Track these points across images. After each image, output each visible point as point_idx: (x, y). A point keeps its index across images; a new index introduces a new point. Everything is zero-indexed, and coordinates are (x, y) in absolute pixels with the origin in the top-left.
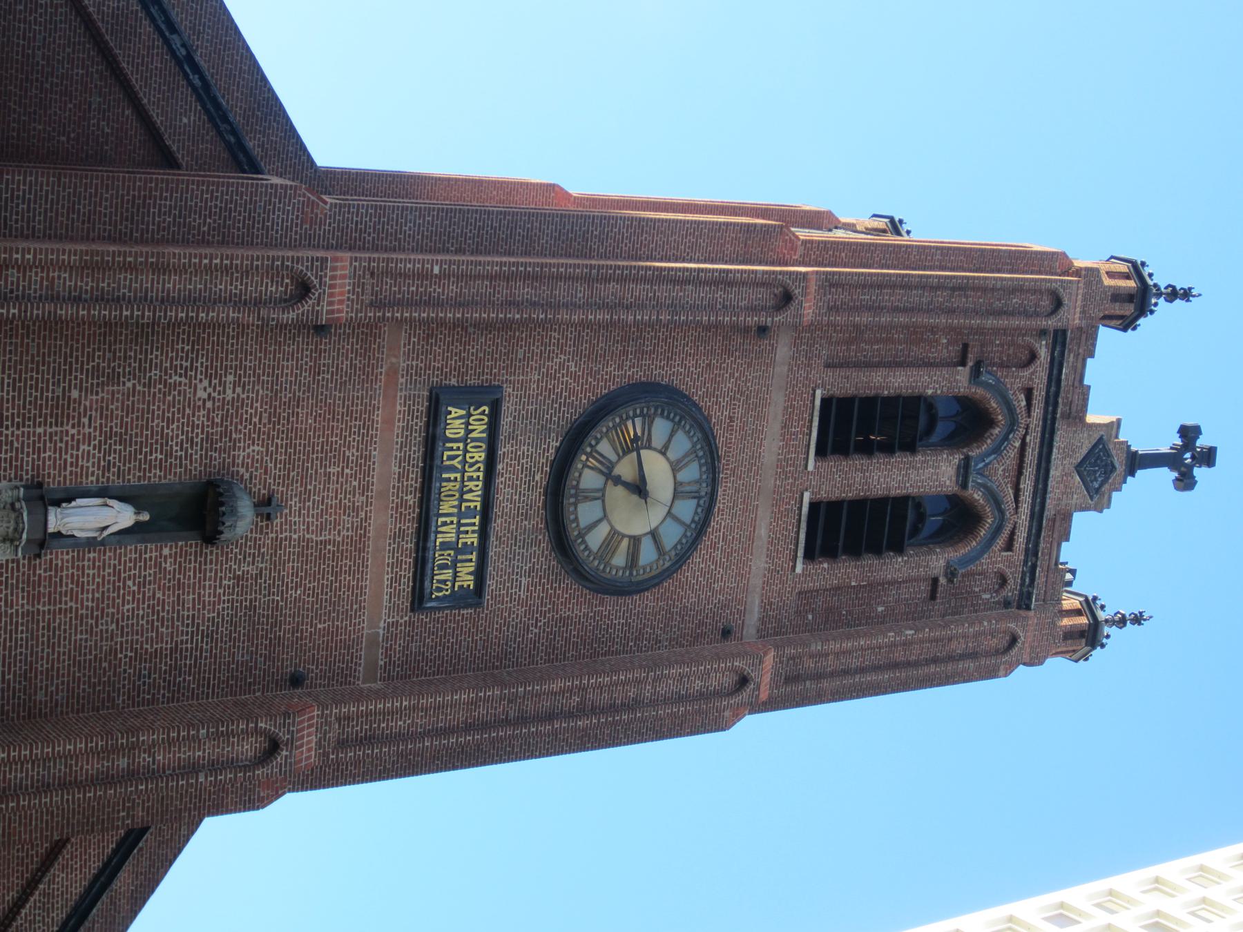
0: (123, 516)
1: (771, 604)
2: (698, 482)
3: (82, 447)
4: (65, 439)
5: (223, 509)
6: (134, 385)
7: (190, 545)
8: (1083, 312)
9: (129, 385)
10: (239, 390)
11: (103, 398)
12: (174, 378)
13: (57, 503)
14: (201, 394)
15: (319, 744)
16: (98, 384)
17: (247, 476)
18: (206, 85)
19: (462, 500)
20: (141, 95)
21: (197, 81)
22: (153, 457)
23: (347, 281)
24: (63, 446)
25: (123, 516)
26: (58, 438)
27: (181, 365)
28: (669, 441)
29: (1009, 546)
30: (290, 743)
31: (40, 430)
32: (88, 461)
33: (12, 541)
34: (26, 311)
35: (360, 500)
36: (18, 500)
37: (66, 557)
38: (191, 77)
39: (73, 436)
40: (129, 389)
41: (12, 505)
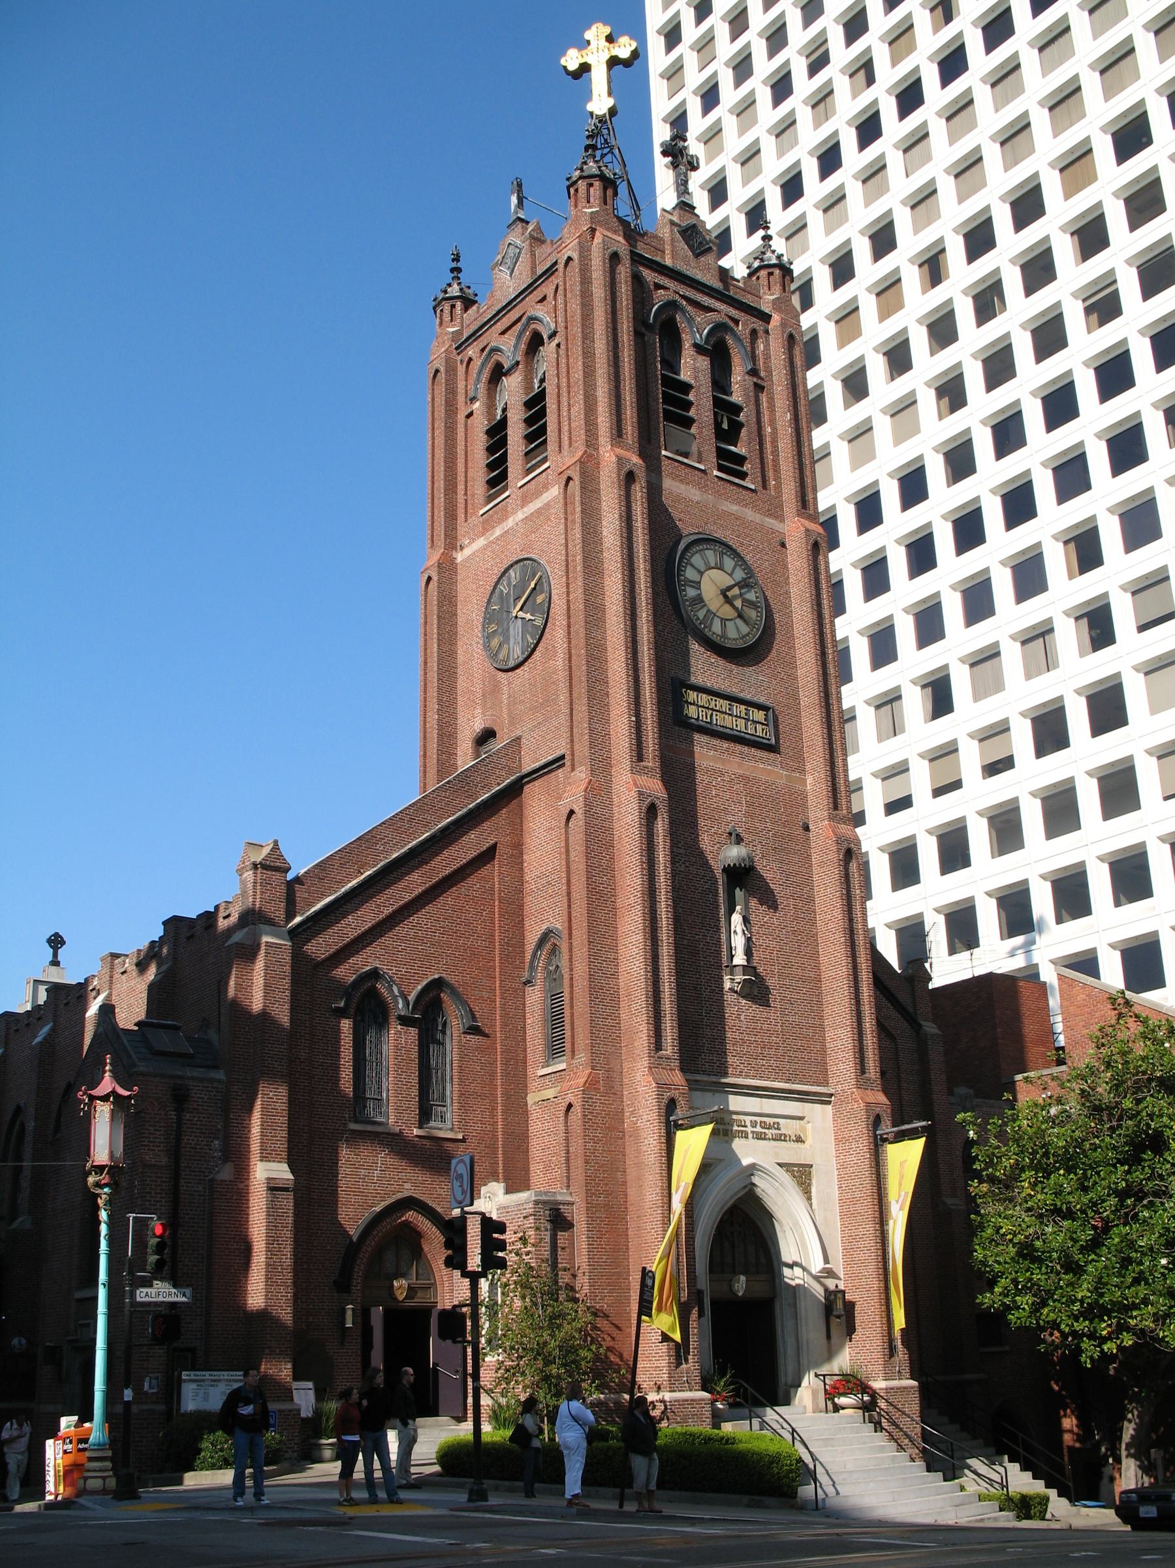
1: (769, 510)
2: (715, 551)
8: (615, 232)
10: (680, 845)
15: (845, 823)
19: (725, 713)
28: (695, 568)
29: (736, 322)
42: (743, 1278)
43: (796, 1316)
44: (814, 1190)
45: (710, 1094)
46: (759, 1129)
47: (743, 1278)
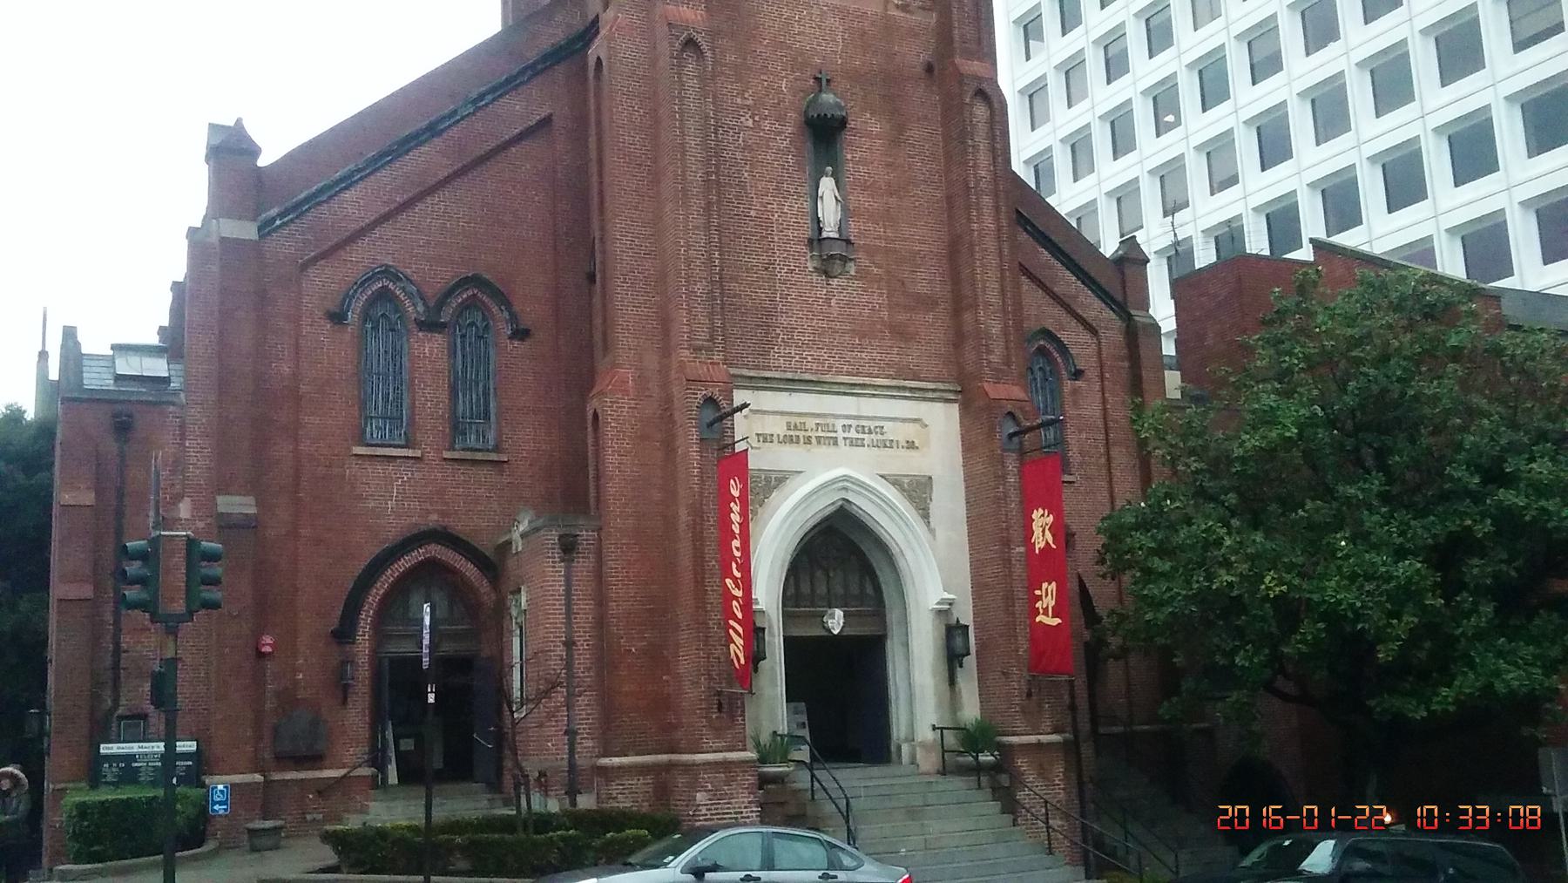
0: (827, 185)
3: (785, 211)
4: (780, 222)
5: (829, 116)
6: (746, 171)
7: (847, 136)
9: (746, 174)
11: (755, 194)
12: (740, 142)
13: (820, 230)
14: (750, 123)
16: (746, 197)
17: (802, 94)
18: (493, 90)
20: (503, 139)
21: (490, 97)
22: (791, 161)
23: (681, 8)
24: (785, 223)
25: (827, 185)
26: (781, 227)
27: (732, 136)
30: (979, 79)
31: (776, 239)
32: (794, 207)
33: (846, 262)
34: (716, 246)
35: (815, 11)
36: (821, 256)
37: (853, 226)
38: (487, 101)
39: (779, 216)
40: (749, 175)
41: (824, 260)
42: (839, 613)
43: (907, 658)
44: (935, 508)
45: (788, 394)
46: (853, 434)
47: (839, 613)
